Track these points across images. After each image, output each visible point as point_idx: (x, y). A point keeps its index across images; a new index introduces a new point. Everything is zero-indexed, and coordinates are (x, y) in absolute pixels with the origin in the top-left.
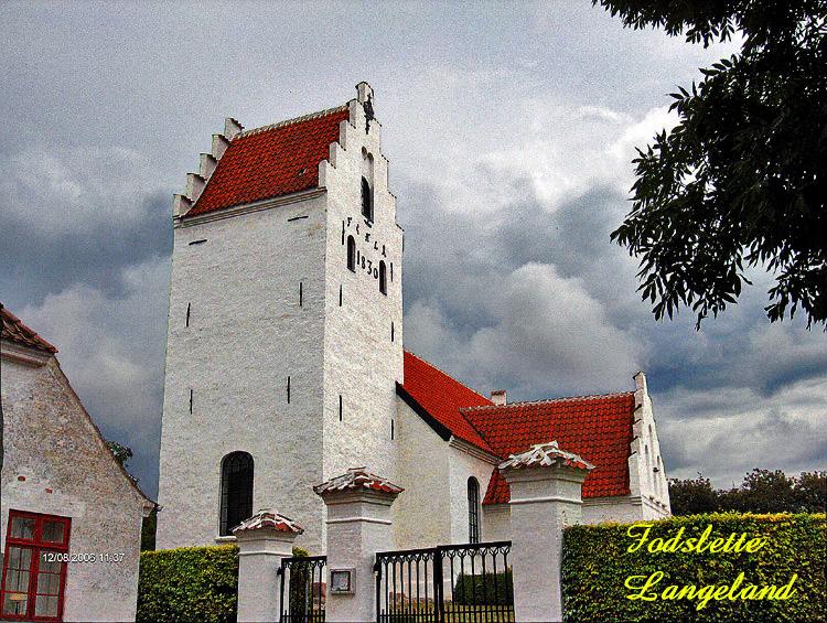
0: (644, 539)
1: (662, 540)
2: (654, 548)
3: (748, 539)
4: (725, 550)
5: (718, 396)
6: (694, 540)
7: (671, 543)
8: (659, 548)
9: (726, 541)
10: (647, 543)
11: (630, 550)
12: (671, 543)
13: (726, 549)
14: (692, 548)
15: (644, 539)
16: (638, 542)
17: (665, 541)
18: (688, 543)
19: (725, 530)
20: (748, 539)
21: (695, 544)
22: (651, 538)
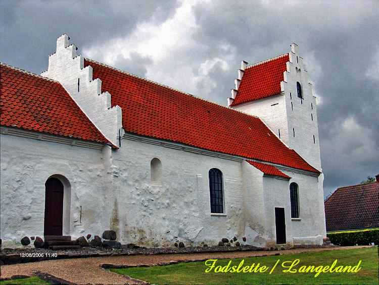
0: (213, 266)
1: (221, 267)
2: (217, 270)
3: (260, 266)
4: (250, 272)
5: (58, 280)
6: (236, 267)
7: (225, 269)
8: (220, 270)
9: (250, 268)
10: (214, 269)
11: (206, 271)
12: (225, 269)
13: (250, 271)
14: (235, 270)
15: (213, 266)
16: (210, 268)
17: (223, 267)
18: (233, 268)
19: (248, 262)
20: (260, 266)
21: (236, 269)
22: (216, 265)
